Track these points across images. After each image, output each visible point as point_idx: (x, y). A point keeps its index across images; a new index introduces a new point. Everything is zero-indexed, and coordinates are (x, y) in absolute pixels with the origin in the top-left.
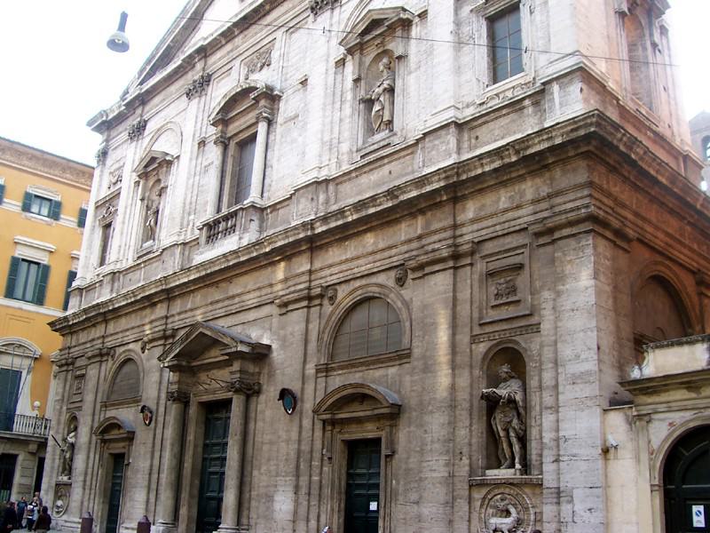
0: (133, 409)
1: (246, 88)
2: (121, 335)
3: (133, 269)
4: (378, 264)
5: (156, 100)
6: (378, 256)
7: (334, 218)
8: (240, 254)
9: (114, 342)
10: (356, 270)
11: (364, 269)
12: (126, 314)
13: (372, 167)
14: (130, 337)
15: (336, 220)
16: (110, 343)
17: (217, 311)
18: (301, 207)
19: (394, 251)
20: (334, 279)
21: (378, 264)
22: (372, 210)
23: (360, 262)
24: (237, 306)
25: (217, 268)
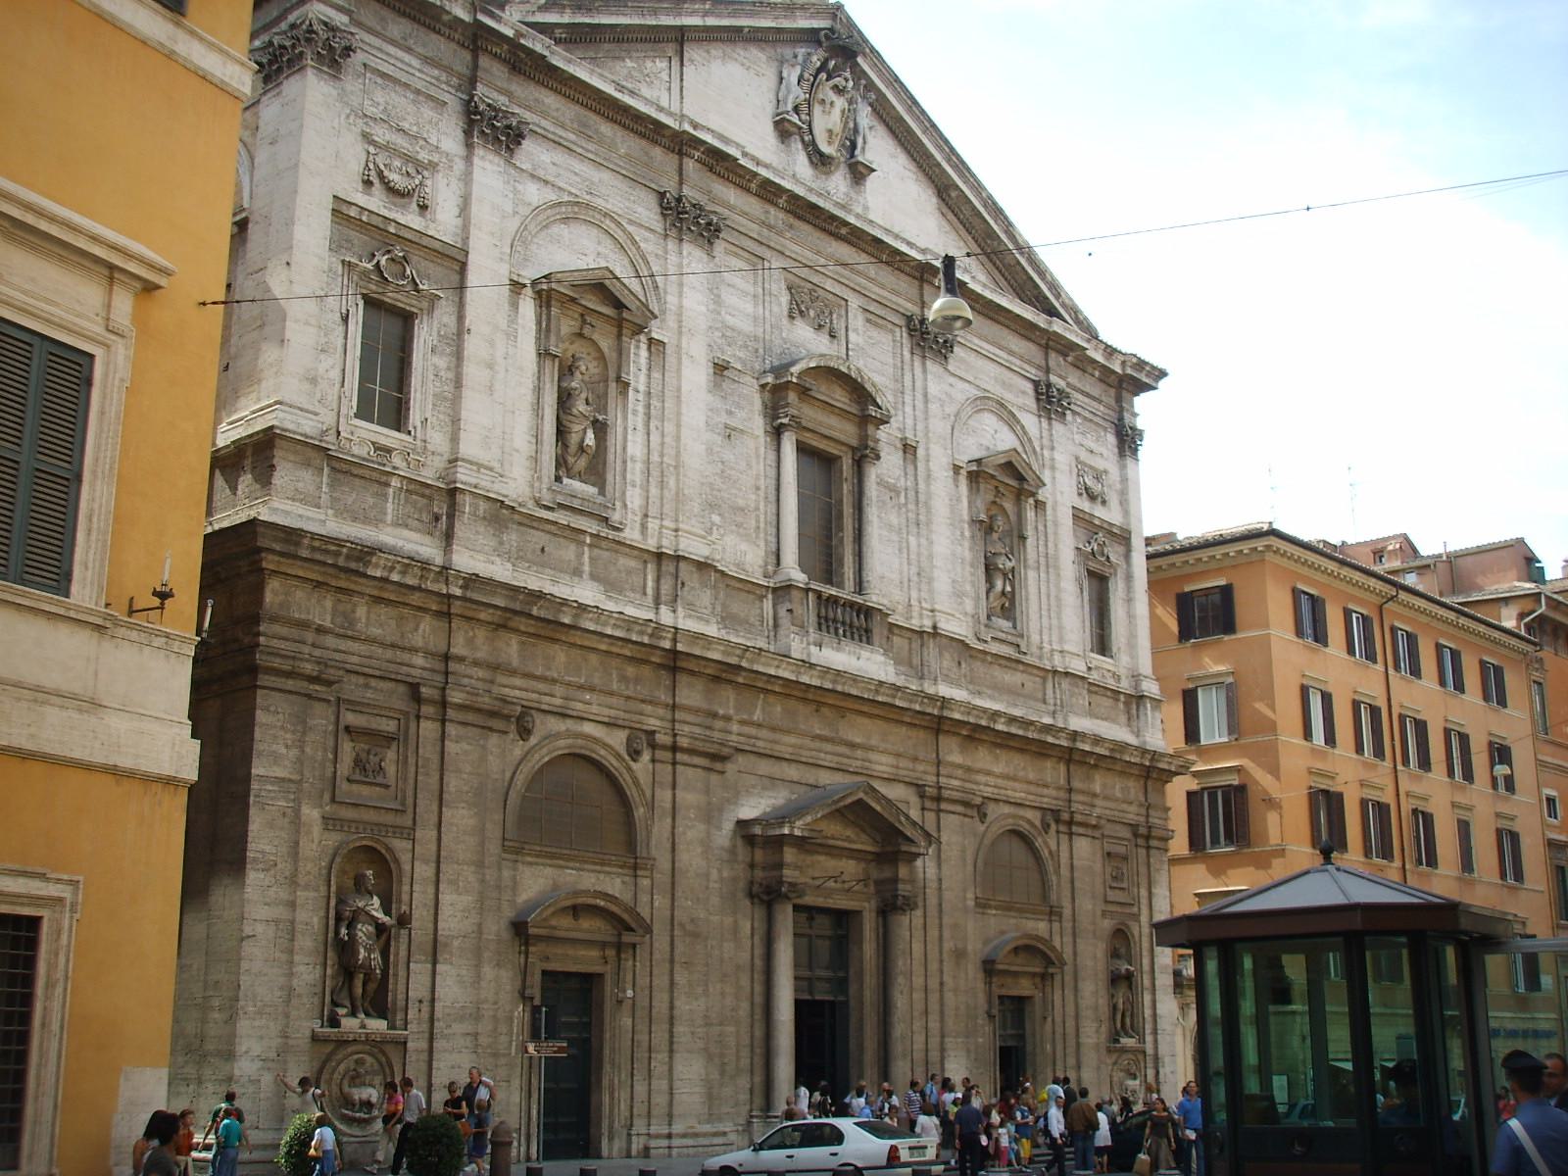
0: (618, 880)
1: (851, 378)
2: (559, 690)
3: (553, 528)
4: (1031, 797)
5: (551, 100)
6: (1032, 788)
7: (1018, 724)
8: (899, 694)
9: (535, 696)
10: (1009, 793)
11: (1019, 796)
12: (573, 645)
13: (1008, 664)
14: (595, 709)
15: (1019, 728)
16: (515, 690)
17: (822, 755)
18: (945, 664)
19: (1046, 791)
20: (988, 791)
21: (1031, 797)
22: (1050, 739)
23: (1017, 785)
24: (859, 763)
25: (854, 692)
